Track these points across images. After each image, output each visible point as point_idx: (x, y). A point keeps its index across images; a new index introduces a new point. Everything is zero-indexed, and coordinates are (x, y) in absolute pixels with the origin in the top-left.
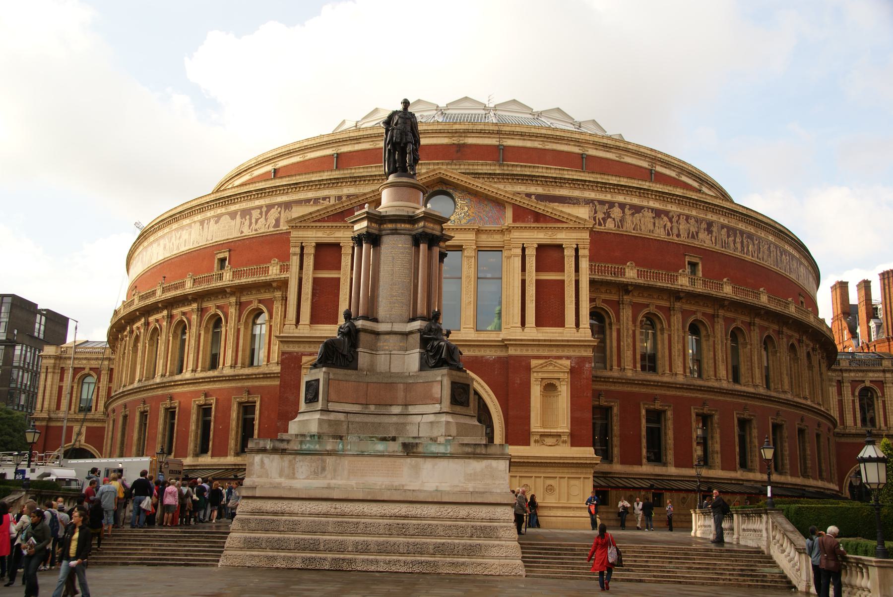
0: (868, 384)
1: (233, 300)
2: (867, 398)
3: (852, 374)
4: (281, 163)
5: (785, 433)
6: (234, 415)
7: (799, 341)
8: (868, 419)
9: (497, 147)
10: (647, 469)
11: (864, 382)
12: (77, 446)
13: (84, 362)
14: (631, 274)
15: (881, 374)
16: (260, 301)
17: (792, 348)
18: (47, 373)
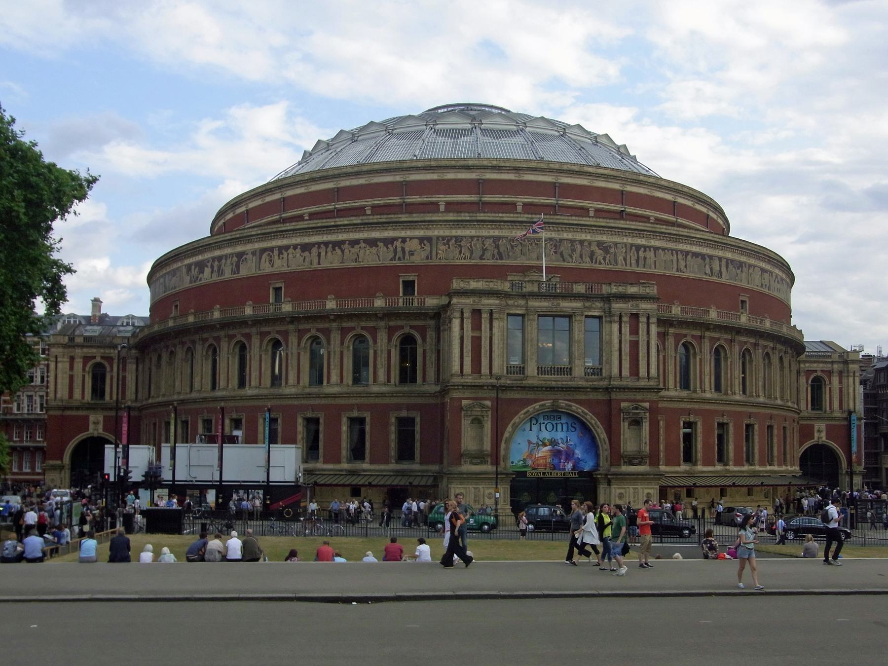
0: (819, 374)
1: (334, 325)
2: (817, 386)
3: (807, 365)
4: (345, 183)
5: (775, 432)
6: (344, 428)
7: (786, 352)
8: (816, 402)
9: (554, 185)
10: (684, 467)
11: (816, 371)
12: (96, 434)
13: (94, 350)
14: (676, 311)
15: (830, 365)
16: (363, 328)
17: (781, 358)
18: (56, 362)
